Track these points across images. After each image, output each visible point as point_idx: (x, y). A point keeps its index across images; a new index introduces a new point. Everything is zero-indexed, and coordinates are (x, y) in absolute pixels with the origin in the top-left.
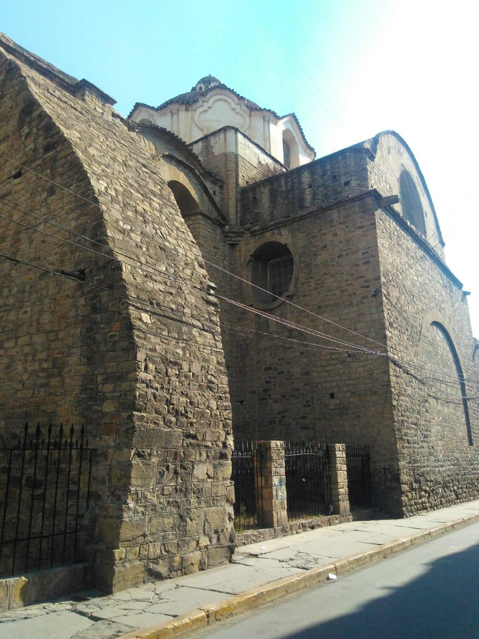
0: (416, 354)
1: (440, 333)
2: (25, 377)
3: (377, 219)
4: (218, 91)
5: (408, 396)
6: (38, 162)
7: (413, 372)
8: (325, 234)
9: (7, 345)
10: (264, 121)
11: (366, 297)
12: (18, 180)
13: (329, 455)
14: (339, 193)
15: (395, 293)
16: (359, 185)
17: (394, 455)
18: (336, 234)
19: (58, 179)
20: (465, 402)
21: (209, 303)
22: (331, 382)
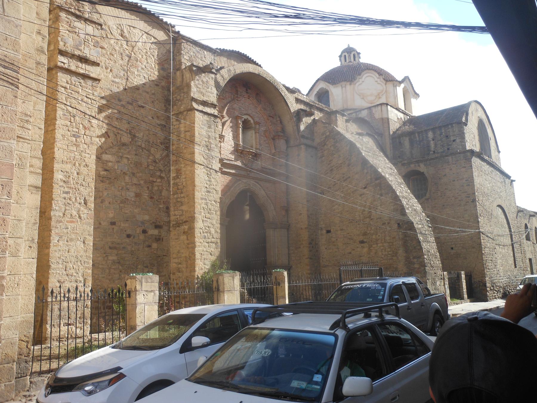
0: (491, 226)
1: (500, 210)
2: (383, 256)
3: (473, 163)
4: (367, 71)
5: (488, 248)
7: (489, 235)
9: (374, 246)
12: (366, 190)
15: (481, 198)
16: (461, 142)
17: (484, 275)
18: (451, 169)
19: (383, 191)
20: (512, 245)
21: (429, 227)
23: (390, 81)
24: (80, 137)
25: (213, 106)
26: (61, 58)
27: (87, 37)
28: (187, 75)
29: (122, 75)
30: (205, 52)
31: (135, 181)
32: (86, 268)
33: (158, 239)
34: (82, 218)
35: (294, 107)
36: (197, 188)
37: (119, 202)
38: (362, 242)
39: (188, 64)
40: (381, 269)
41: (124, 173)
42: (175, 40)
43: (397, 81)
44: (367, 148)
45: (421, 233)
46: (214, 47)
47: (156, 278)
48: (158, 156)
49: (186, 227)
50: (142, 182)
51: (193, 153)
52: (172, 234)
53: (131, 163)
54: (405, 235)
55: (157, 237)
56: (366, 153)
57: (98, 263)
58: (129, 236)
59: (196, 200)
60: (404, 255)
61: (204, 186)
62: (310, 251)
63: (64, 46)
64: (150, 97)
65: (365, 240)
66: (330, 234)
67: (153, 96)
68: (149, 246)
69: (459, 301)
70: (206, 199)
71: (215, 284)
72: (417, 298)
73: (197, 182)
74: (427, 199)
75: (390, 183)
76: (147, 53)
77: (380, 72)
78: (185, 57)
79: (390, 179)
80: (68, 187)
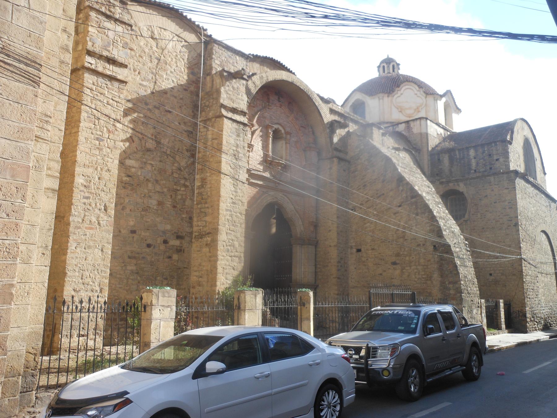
0: (533, 252)
1: (544, 235)
2: (416, 280)
3: (517, 185)
4: (407, 83)
6: (409, 202)
7: (531, 262)
8: (486, 189)
9: (406, 268)
10: (434, 100)
11: (510, 226)
12: (400, 208)
13: (497, 306)
14: (492, 164)
15: (524, 222)
16: (504, 161)
17: (524, 305)
18: (493, 190)
21: (468, 251)
22: (490, 268)
23: (430, 94)
24: (103, 140)
25: (243, 113)
26: (88, 59)
27: (116, 37)
28: (218, 80)
29: (150, 78)
30: (238, 57)
31: (158, 188)
32: (103, 277)
33: (179, 250)
34: (102, 225)
35: (328, 118)
36: (222, 199)
37: (140, 209)
38: (394, 263)
39: (219, 69)
40: (414, 293)
41: (147, 180)
42: (207, 43)
43: (438, 94)
44: (404, 164)
45: (458, 257)
46: (247, 52)
47: (174, 293)
48: (183, 164)
49: (209, 239)
50: (165, 190)
51: (220, 162)
52: (194, 245)
53: (155, 169)
54: (442, 259)
55: (179, 248)
56: (403, 169)
57: (116, 273)
58: (149, 246)
59: (220, 211)
60: (440, 279)
61: (229, 197)
62: (338, 270)
63: (93, 46)
64: (178, 102)
65: (398, 262)
66: (360, 253)
67: (181, 101)
68: (170, 257)
69: (496, 331)
70: (231, 211)
71: (236, 302)
72: (453, 328)
73: (223, 192)
74: (466, 221)
75: (427, 202)
76: (177, 56)
77: (420, 85)
78: (216, 61)
79: (427, 198)
80: (88, 192)
